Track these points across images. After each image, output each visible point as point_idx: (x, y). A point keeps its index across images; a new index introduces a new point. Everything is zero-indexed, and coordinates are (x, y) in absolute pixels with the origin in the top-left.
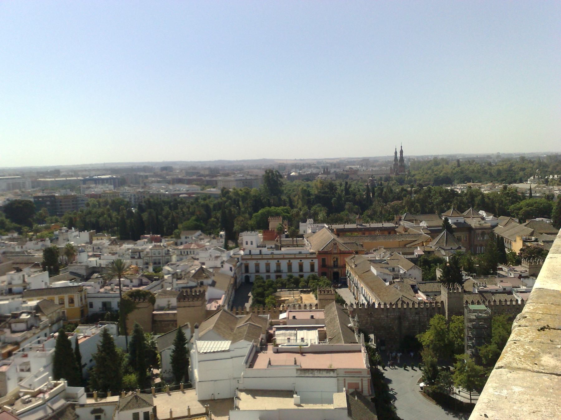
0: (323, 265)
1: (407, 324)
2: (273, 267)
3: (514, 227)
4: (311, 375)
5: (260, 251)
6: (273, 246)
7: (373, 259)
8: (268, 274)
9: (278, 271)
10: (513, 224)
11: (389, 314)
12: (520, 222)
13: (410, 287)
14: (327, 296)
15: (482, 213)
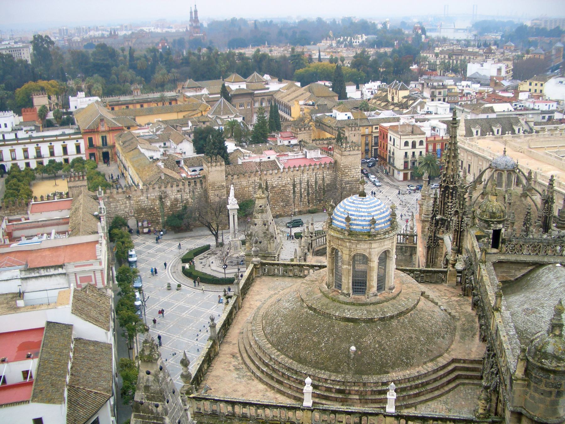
0: (91, 144)
1: (168, 204)
2: (32, 152)
3: (294, 91)
4: (37, 275)
5: (16, 135)
6: (33, 128)
7: (147, 134)
8: (27, 161)
9: (39, 155)
10: (294, 88)
11: (149, 195)
12: (302, 86)
13: (175, 163)
14: (79, 182)
15: (267, 77)
